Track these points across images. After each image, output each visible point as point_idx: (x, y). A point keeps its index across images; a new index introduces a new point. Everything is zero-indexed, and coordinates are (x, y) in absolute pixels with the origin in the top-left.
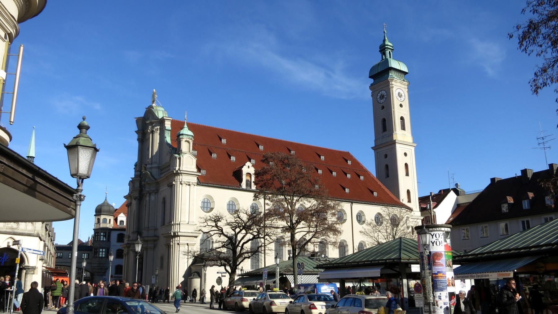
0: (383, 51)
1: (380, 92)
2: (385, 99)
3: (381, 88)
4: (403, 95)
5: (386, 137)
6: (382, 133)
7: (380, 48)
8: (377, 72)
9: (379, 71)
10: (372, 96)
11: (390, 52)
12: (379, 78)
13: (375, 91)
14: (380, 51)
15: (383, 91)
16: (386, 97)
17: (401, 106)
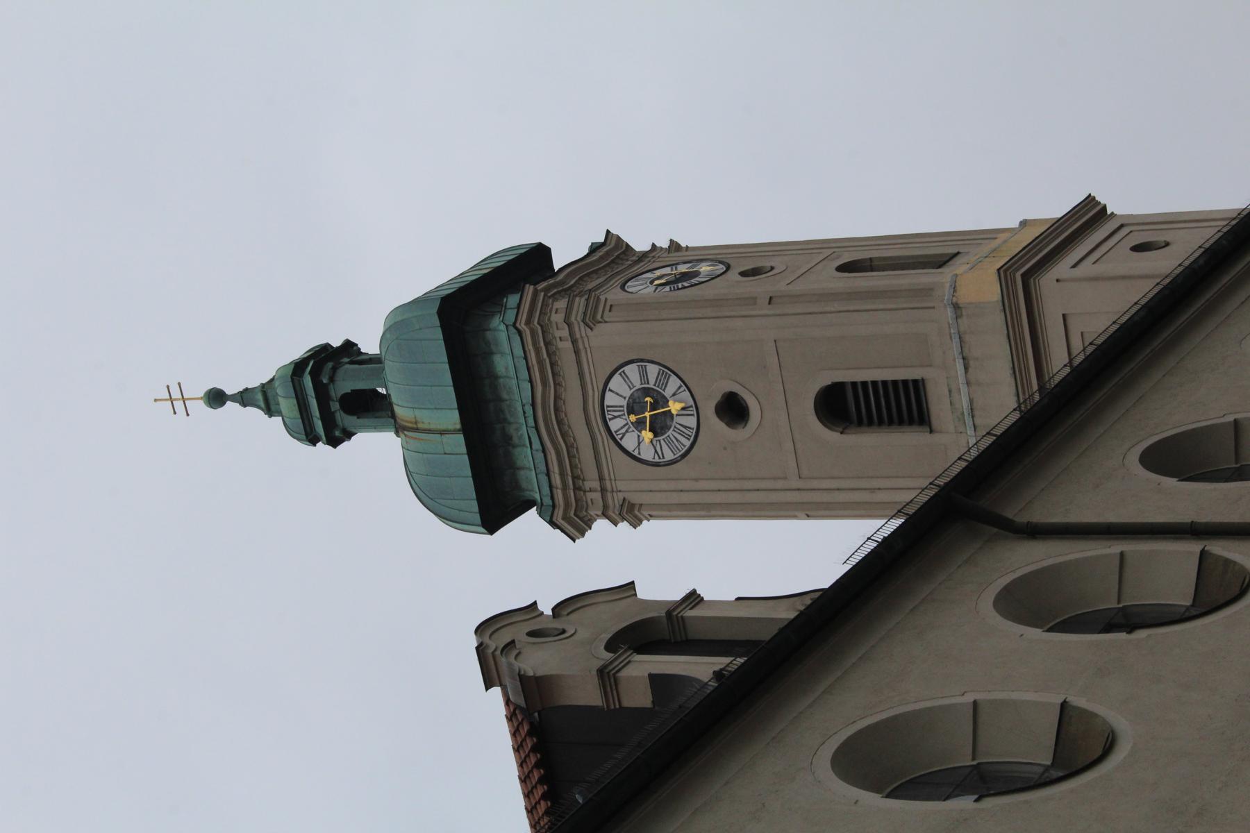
0: (335, 406)
1: (615, 425)
2: (674, 383)
3: (588, 424)
4: (683, 268)
5: (968, 383)
6: (931, 431)
7: (313, 440)
8: (460, 438)
9: (452, 418)
10: (631, 513)
11: (352, 363)
12: (507, 439)
13: (601, 478)
14: (334, 442)
15: (610, 399)
16: (653, 370)
17: (754, 272)
